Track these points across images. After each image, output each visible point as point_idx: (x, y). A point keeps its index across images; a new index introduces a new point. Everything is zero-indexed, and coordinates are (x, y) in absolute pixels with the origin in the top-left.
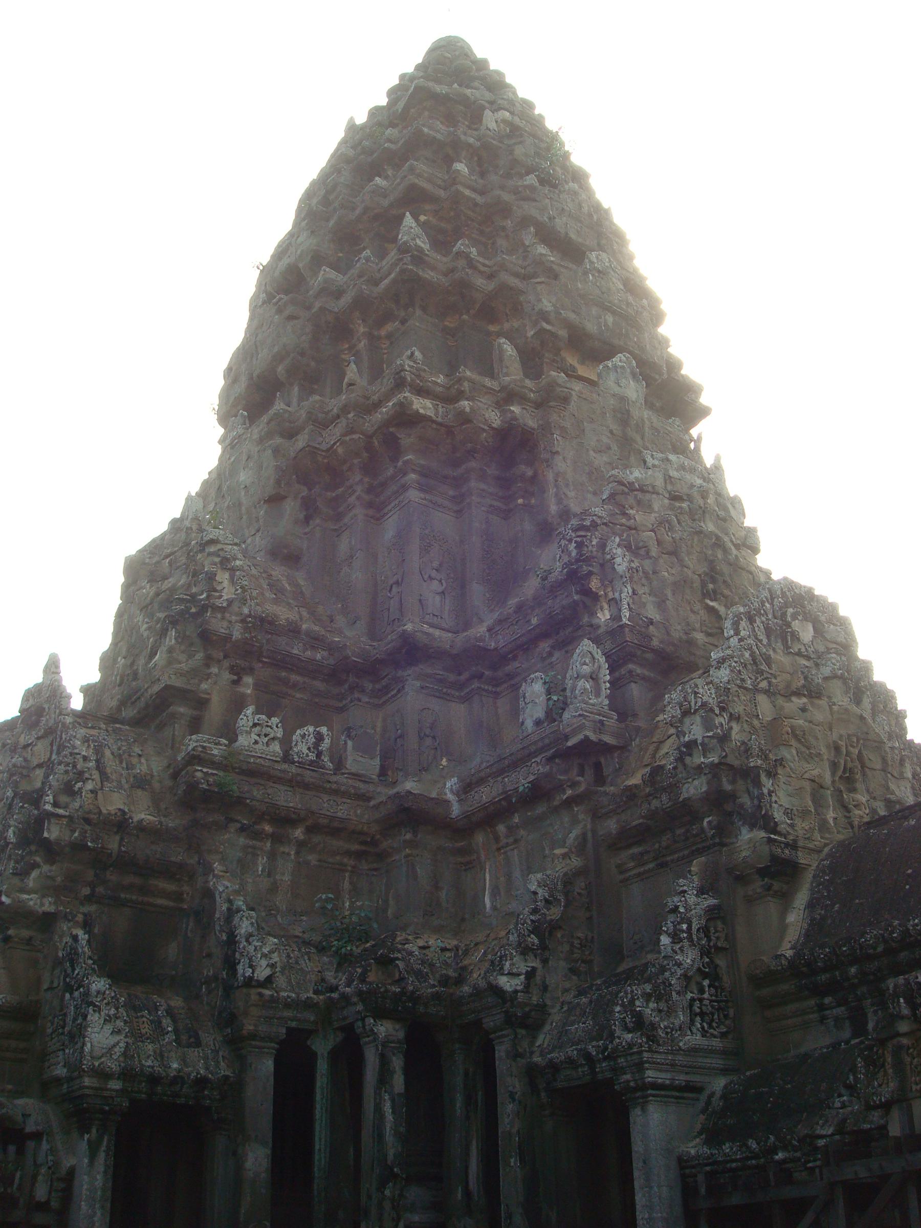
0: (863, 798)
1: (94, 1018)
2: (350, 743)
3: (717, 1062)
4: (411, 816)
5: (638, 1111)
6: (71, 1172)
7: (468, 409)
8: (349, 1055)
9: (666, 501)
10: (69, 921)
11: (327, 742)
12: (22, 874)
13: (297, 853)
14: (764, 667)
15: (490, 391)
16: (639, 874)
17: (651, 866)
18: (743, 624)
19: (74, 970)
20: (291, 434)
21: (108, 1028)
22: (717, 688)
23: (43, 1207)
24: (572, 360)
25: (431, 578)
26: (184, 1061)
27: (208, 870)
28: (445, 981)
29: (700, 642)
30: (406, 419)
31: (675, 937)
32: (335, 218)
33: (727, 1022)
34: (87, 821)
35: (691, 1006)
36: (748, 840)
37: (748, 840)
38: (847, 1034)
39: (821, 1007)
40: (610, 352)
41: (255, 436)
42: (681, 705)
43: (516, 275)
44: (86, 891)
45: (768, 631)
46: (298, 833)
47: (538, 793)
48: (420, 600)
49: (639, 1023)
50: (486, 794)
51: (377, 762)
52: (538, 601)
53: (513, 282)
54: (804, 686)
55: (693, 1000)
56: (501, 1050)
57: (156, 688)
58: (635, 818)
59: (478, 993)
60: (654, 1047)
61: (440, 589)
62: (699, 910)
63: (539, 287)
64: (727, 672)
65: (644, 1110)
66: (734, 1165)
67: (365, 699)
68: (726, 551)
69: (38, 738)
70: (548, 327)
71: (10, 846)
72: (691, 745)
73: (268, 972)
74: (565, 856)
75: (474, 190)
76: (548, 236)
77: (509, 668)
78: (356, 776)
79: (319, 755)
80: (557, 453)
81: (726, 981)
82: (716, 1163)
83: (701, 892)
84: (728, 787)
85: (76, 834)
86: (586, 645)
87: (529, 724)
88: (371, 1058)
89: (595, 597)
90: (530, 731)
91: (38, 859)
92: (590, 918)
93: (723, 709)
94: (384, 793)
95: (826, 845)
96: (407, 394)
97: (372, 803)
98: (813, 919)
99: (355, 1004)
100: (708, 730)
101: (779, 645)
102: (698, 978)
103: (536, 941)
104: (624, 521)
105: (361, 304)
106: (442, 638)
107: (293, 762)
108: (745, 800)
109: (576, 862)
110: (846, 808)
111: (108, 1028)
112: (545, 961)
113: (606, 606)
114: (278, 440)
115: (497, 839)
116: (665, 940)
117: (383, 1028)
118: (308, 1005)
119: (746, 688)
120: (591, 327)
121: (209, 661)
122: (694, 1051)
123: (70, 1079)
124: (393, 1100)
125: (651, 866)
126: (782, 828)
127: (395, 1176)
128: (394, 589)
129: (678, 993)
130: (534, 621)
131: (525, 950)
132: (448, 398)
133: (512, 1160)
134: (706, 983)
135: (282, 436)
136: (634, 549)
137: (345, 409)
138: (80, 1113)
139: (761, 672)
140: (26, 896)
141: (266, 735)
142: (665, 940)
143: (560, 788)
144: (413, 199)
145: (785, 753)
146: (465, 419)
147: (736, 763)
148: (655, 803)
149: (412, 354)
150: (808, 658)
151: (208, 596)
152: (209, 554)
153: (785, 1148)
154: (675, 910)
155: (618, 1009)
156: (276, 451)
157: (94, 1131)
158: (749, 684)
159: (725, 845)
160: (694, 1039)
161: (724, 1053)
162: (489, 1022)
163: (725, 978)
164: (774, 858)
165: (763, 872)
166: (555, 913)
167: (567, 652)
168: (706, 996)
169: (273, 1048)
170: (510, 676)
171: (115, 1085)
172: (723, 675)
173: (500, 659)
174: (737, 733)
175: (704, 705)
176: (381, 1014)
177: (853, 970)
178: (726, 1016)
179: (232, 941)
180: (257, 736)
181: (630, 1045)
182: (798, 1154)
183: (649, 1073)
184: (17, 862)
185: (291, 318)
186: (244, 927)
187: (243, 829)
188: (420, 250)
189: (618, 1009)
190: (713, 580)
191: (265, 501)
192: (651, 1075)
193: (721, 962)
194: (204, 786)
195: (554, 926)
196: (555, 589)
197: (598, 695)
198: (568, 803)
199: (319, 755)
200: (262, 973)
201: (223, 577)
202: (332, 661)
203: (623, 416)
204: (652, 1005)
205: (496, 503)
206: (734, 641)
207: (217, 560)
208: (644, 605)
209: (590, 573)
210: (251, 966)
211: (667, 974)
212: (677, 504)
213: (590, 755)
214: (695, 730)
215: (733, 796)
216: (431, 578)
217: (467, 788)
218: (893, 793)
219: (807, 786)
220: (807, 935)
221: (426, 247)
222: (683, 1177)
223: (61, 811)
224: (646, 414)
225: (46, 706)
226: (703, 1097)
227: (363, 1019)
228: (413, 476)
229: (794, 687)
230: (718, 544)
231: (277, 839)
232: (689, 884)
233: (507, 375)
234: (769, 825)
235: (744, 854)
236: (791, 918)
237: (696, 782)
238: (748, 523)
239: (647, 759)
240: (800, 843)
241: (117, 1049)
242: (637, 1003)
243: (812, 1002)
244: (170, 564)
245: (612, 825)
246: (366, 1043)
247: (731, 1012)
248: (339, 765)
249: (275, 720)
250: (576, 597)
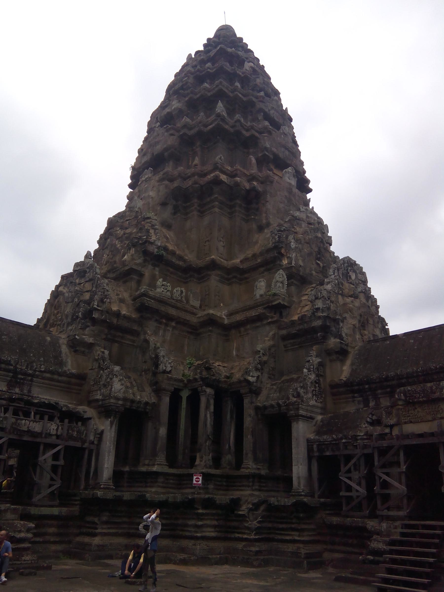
0: (366, 332)
1: (115, 379)
2: (191, 295)
3: (319, 411)
4: (211, 322)
5: (295, 423)
6: (102, 432)
7: (239, 181)
8: (194, 400)
9: (306, 224)
10: (99, 346)
11: (184, 294)
12: (83, 329)
13: (172, 330)
14: (341, 286)
15: (245, 175)
16: (292, 349)
17: (297, 346)
18: (336, 271)
19: (104, 363)
20: (171, 180)
21: (120, 383)
22: (327, 292)
23: (92, 443)
24: (272, 167)
25: (220, 241)
26: (141, 396)
27: (145, 333)
28: (228, 377)
29: (314, 275)
30: (217, 182)
31: (309, 370)
32: (189, 97)
33: (322, 399)
34: (107, 312)
35: (313, 392)
36: (333, 342)
37: (333, 342)
38: (362, 406)
39: (354, 397)
40: (287, 166)
41: (157, 179)
42: (315, 296)
43: (257, 131)
44: (104, 337)
45: (343, 274)
46: (173, 324)
47: (259, 318)
48: (217, 248)
49: (298, 395)
50: (239, 317)
51: (199, 302)
52: (261, 254)
53: (257, 134)
54: (353, 294)
55: (313, 390)
56: (246, 401)
57: (127, 268)
58: (293, 331)
59: (240, 382)
60: (303, 403)
61: (223, 245)
62: (316, 362)
63: (266, 138)
64: (331, 286)
65: (297, 423)
66: (327, 443)
67: (195, 280)
68: (324, 244)
69: (86, 282)
70: (267, 154)
71: (79, 319)
72: (318, 309)
73: (170, 369)
74: (269, 340)
75: (242, 94)
76: (267, 117)
77: (246, 275)
78: (192, 306)
79: (182, 298)
80: (268, 201)
81: (322, 386)
82: (320, 442)
83: (317, 356)
84: (328, 324)
85: (104, 317)
86: (281, 271)
87: (258, 296)
88: (203, 400)
89: (282, 255)
90: (258, 298)
91: (89, 324)
92: (275, 361)
93: (329, 299)
94: (201, 314)
95: (356, 346)
96: (218, 173)
97: (197, 316)
98: (353, 369)
99: (199, 381)
100: (324, 305)
101: (345, 280)
102: (315, 384)
103: (260, 367)
104: (293, 230)
105: (200, 134)
106: (225, 263)
107: (174, 299)
108: (334, 329)
109: (272, 343)
110: (361, 335)
111: (120, 383)
112: (262, 374)
113: (286, 259)
114: (166, 182)
115: (240, 332)
116: (305, 370)
117: (209, 390)
118: (182, 381)
119: (336, 293)
120: (281, 155)
121: (145, 261)
122: (313, 406)
123: (102, 400)
124: (210, 413)
125: (297, 346)
126: (345, 339)
127: (210, 438)
128: (207, 243)
129: (310, 387)
130: (259, 260)
131: (257, 369)
132: (232, 175)
133: (249, 436)
134: (317, 385)
135: (168, 181)
136: (297, 241)
137: (193, 175)
138: (106, 411)
139: (340, 288)
140: (84, 337)
141: (166, 289)
142: (305, 370)
143: (267, 318)
144: (220, 95)
145: (346, 315)
146: (237, 184)
147: (332, 316)
148: (301, 327)
149: (221, 157)
150: (354, 285)
151: (147, 238)
152: (147, 222)
153: (346, 438)
154: (309, 361)
155: (291, 390)
156: (166, 187)
157: (112, 418)
158: (336, 291)
159: (325, 342)
160: (312, 402)
161: (321, 408)
162: (242, 391)
163: (322, 385)
164: (342, 349)
165: (337, 353)
166: (265, 358)
167: (270, 273)
168: (317, 389)
170: (246, 278)
171: (120, 402)
172: (329, 287)
173: (242, 272)
174: (333, 307)
175: (323, 297)
176: (208, 385)
177: (367, 386)
178: (322, 397)
179: (157, 357)
180: (163, 288)
181: (295, 402)
182: (350, 441)
183: (300, 411)
184: (82, 324)
185: (172, 135)
186: (162, 353)
187: (156, 320)
188: (224, 117)
189: (291, 390)
190: (319, 254)
191: (160, 204)
192: (301, 412)
193: (321, 380)
194: (147, 304)
195: (265, 362)
196: (268, 251)
197: (283, 288)
198: (269, 323)
199: (182, 298)
200: (169, 369)
201: (152, 231)
202: (185, 266)
203: (290, 191)
204: (302, 390)
205: (243, 217)
206: (333, 276)
207: (150, 225)
208: (299, 260)
209: (282, 247)
210: (165, 366)
211: (306, 381)
212: (310, 226)
213: (280, 309)
214: (319, 304)
215: (329, 327)
216: (220, 241)
217: (230, 315)
218: (375, 332)
219: (352, 326)
220: (351, 374)
221: (226, 115)
222: (308, 445)
223: (99, 308)
224: (297, 190)
225: (88, 270)
226: (315, 421)
227: (201, 387)
228: (217, 203)
229: (350, 294)
230: (322, 242)
231: (166, 325)
232: (313, 353)
233: (252, 170)
234: (341, 337)
235: (331, 346)
236: (345, 368)
237: (318, 321)
238: (329, 235)
239: (299, 312)
240: (349, 345)
241: (122, 391)
242: (298, 389)
243: (350, 395)
244: (129, 223)
245: (284, 332)
246: (202, 395)
247: (323, 396)
248: (188, 301)
249: (169, 284)
250: (276, 255)
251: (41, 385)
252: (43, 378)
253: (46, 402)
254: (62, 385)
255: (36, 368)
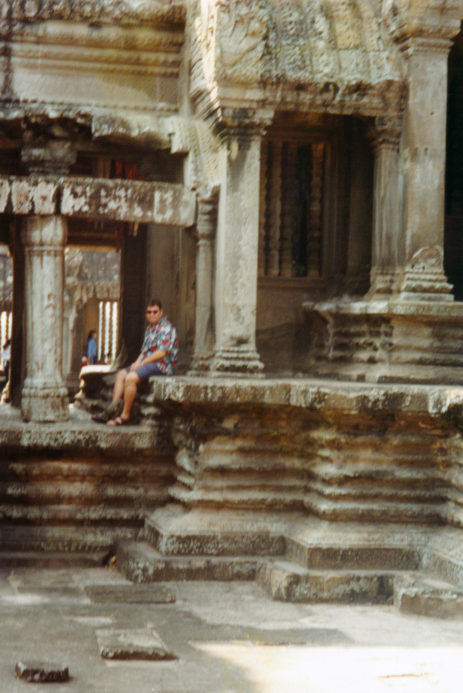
169: (445, 46)
171: (255, 94)
251: (39, 61)
252: (39, 41)
253: (53, 114)
254: (111, 53)
255: (10, 12)
